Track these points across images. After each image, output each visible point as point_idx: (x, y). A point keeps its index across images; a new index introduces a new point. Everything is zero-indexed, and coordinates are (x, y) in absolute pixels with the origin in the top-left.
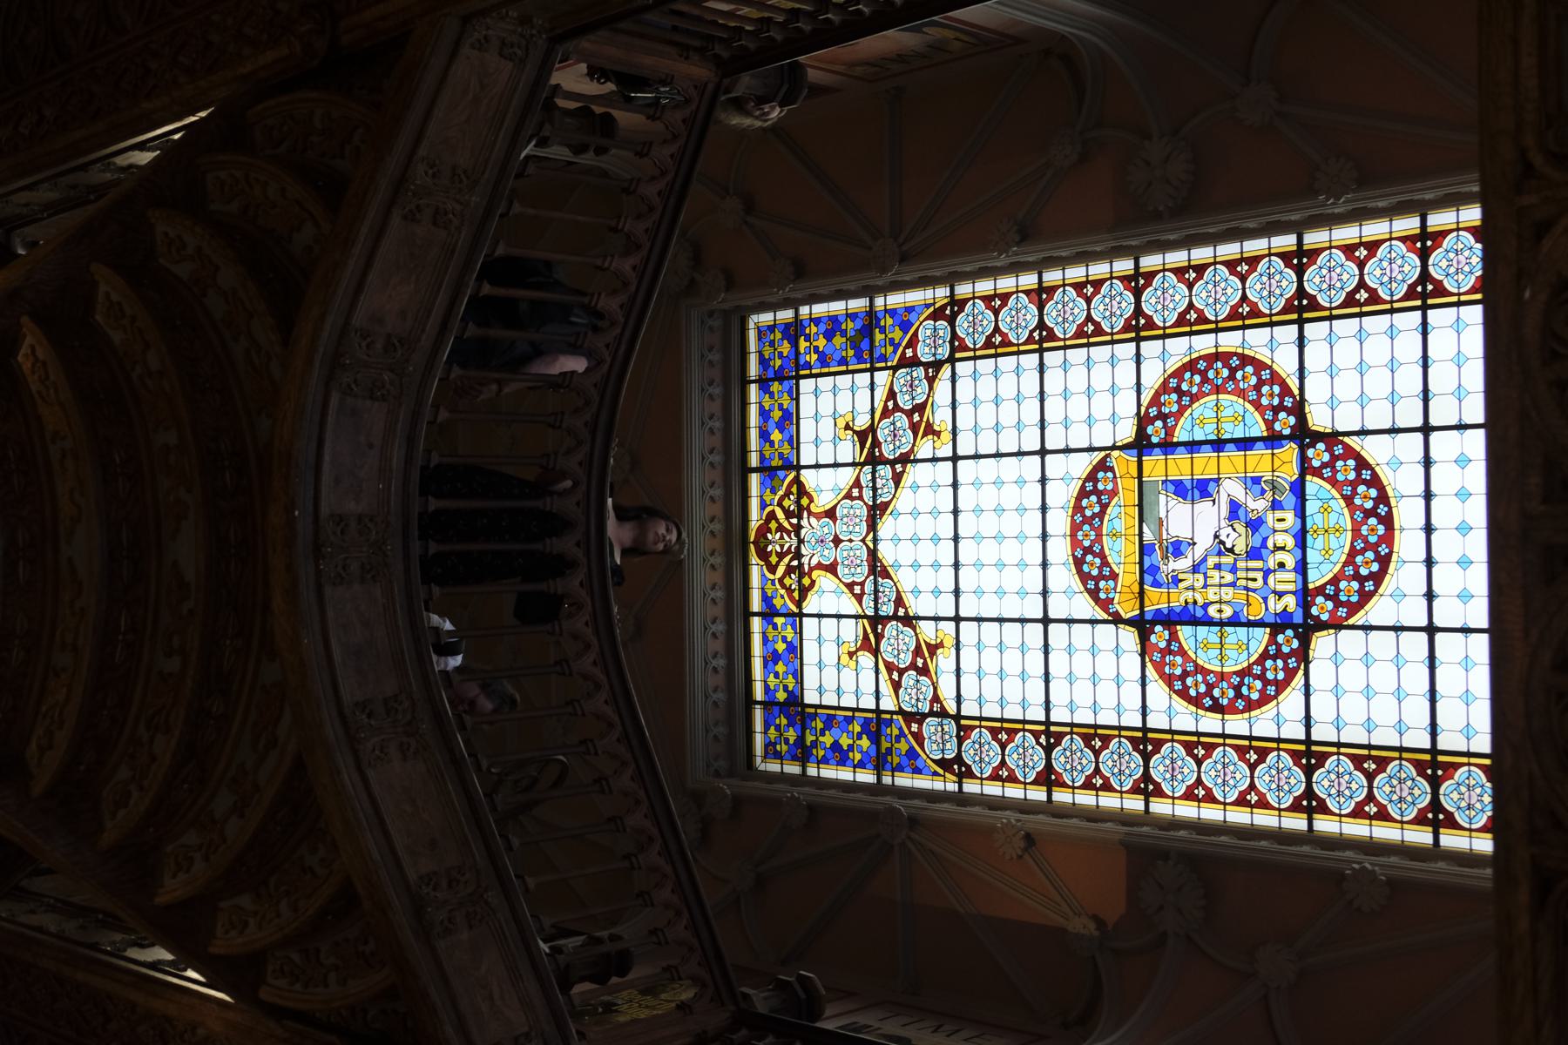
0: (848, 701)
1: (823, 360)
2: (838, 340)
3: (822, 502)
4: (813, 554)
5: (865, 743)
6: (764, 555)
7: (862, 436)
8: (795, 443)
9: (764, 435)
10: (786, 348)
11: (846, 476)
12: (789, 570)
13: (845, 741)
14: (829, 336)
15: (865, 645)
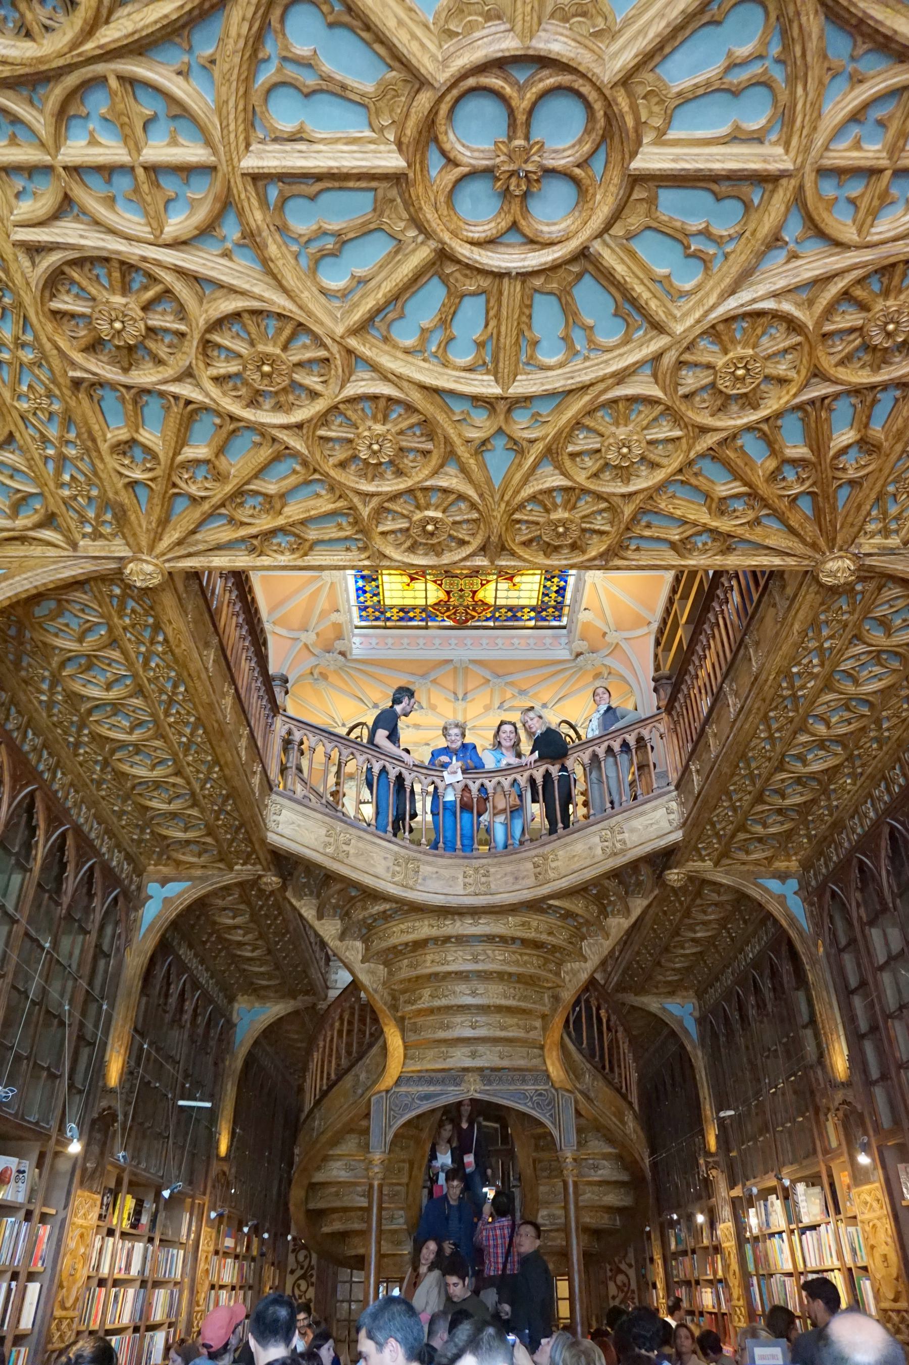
0: (536, 587)
1: (377, 595)
2: (367, 588)
3: (442, 595)
4: (469, 601)
5: (556, 580)
6: (467, 621)
7: (412, 579)
8: (414, 608)
9: (411, 619)
10: (370, 610)
11: (431, 586)
12: (474, 610)
13: (555, 588)
14: (365, 592)
15: (511, 579)
